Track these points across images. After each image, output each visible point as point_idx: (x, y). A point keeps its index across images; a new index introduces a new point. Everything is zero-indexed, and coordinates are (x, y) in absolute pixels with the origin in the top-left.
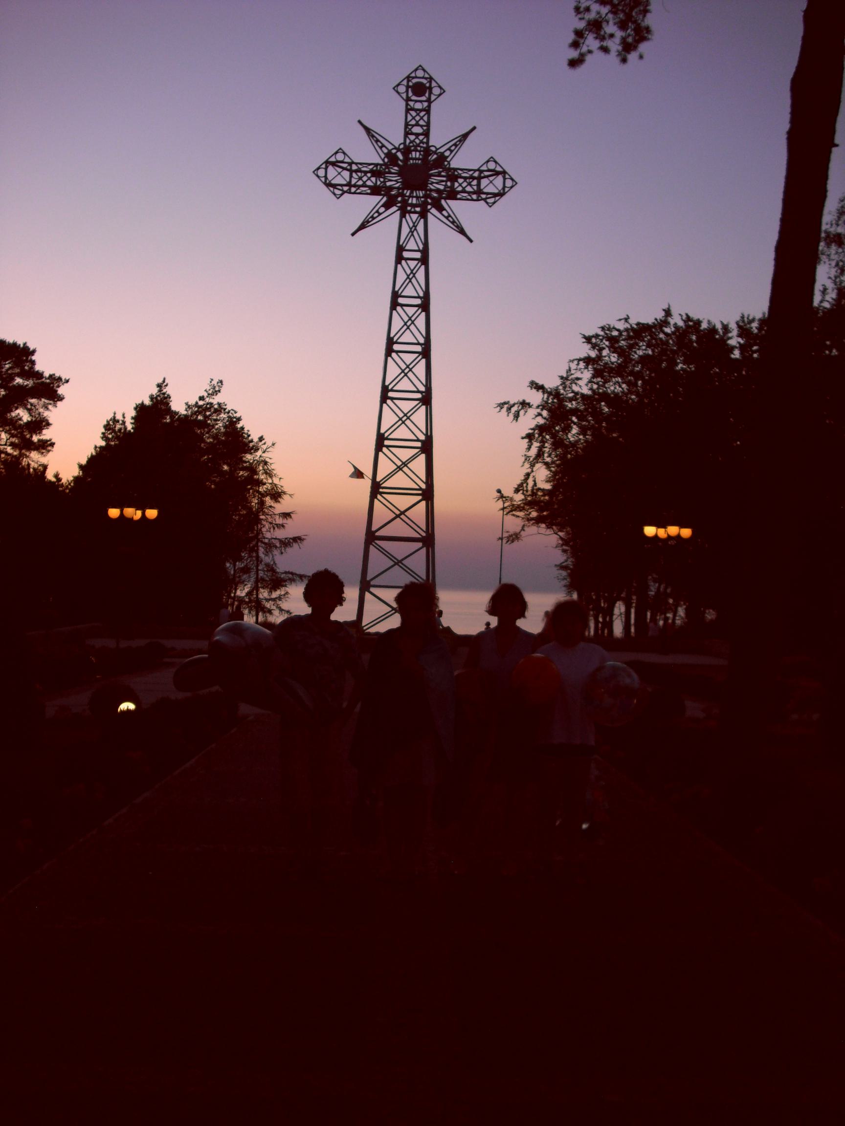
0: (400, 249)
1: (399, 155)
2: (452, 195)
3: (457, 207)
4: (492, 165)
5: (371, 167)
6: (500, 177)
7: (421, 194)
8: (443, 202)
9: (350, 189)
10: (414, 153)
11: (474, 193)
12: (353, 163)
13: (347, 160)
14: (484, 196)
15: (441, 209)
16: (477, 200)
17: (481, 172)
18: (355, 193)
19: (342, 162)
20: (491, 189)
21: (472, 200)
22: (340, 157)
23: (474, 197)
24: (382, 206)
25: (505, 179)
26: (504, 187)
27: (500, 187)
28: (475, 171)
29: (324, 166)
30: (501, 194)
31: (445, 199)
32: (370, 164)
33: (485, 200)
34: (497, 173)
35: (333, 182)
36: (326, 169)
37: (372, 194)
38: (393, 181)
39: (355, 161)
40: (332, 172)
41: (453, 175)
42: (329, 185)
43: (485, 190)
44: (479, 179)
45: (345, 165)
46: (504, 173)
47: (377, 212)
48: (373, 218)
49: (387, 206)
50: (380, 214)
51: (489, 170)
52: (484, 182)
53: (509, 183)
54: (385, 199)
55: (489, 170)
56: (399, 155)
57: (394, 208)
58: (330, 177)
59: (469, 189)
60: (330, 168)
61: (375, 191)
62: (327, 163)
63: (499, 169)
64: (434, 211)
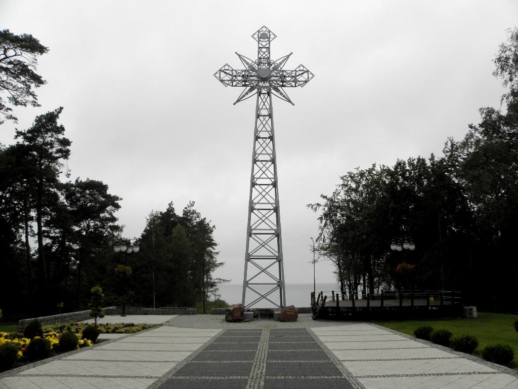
3: (287, 90)
4: (301, 68)
6: (306, 74)
12: (233, 70)
15: (277, 90)
16: (295, 86)
18: (236, 86)
19: (228, 70)
21: (292, 86)
22: (227, 67)
26: (308, 78)
30: (306, 82)
34: (305, 72)
40: (223, 74)
42: (222, 81)
45: (227, 72)
46: (308, 71)
53: (310, 76)
55: (300, 71)
58: (222, 77)
60: (222, 73)
62: (220, 70)
63: (305, 70)
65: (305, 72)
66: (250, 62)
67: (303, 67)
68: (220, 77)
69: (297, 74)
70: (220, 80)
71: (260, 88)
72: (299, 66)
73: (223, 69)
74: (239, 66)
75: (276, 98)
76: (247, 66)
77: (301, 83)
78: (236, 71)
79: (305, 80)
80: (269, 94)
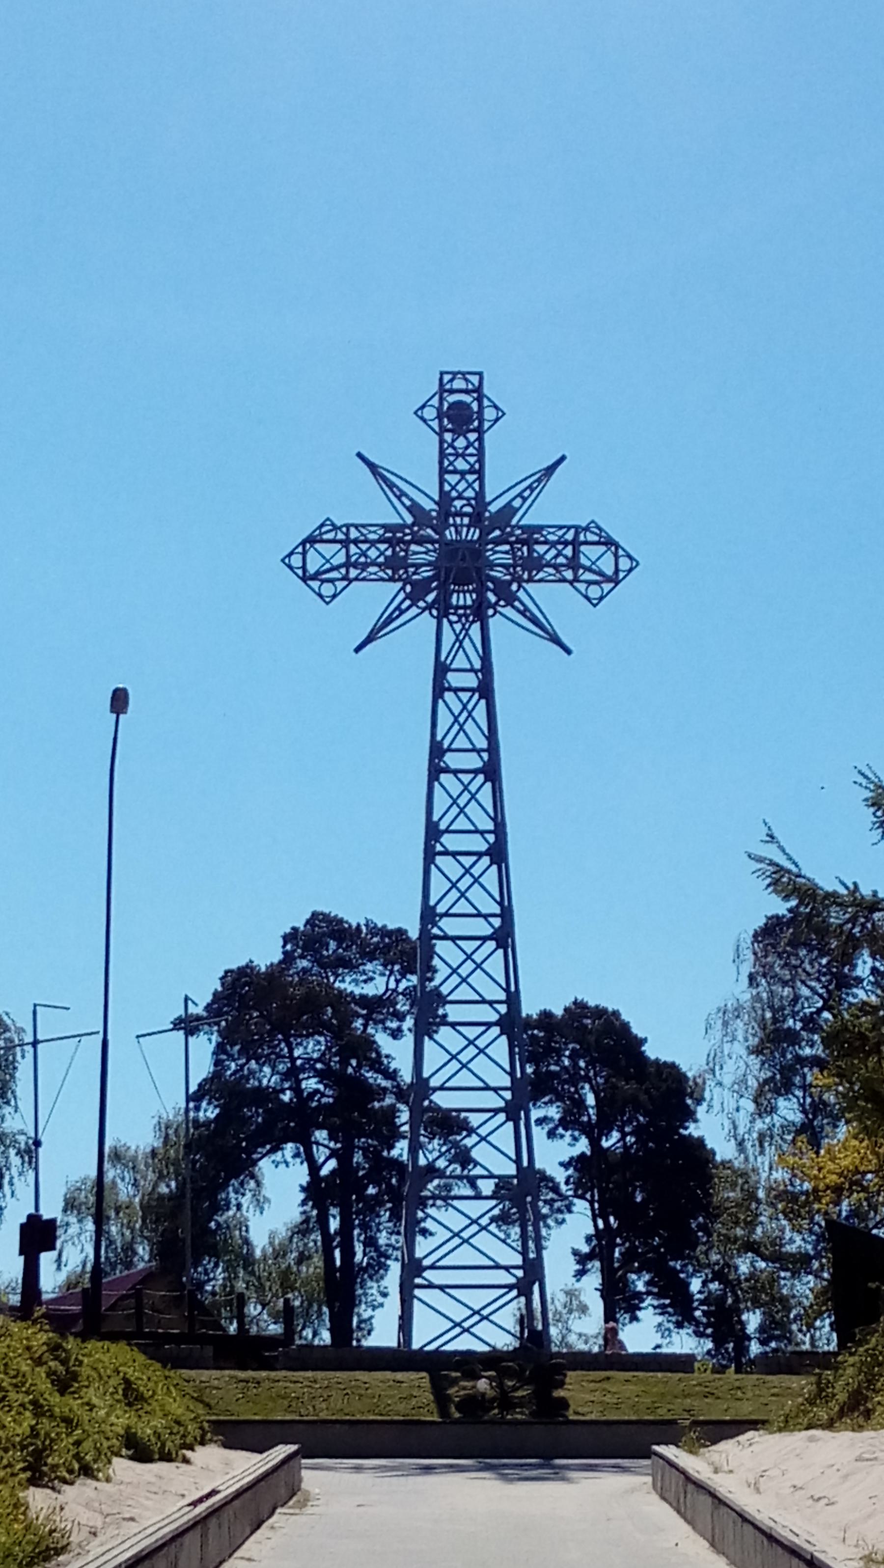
0: (441, 669)
1: (492, 598)
2: (393, 535)
3: (383, 512)
4: (327, 590)
5: (541, 575)
6: (312, 569)
7: (450, 534)
8: (409, 520)
9: (577, 534)
10: (469, 602)
11: (356, 542)
12: (571, 583)
13: (582, 587)
14: (341, 536)
15: (414, 508)
16: (348, 526)
18: (569, 528)
19: (590, 583)
20: (328, 550)
21: (356, 527)
22: (594, 592)
23: (354, 534)
24: (518, 509)
25: (304, 568)
26: (304, 554)
27: (311, 554)
28: (356, 579)
29: (621, 575)
30: (311, 540)
31: (404, 526)
32: (541, 580)
33: (335, 528)
35: (603, 548)
36: (617, 571)
37: (539, 529)
38: (500, 555)
39: (567, 585)
41: (395, 567)
42: (609, 543)
43: (339, 546)
44: (347, 565)
46: (305, 579)
47: (525, 499)
48: (530, 488)
49: (509, 510)
50: (520, 495)
51: (332, 581)
52: (341, 558)
53: (296, 561)
54: (514, 522)
55: (332, 581)
56: (492, 598)
57: (493, 508)
58: (609, 557)
59: (364, 547)
60: (609, 571)
61: (532, 535)
62: (615, 580)
63: (315, 584)
64: (428, 505)
65: (314, 577)
66: (508, 611)
67: (320, 596)
68: (616, 556)
69: (343, 571)
70: (617, 546)
71: (476, 519)
72: (334, 596)
73: (607, 587)
74: (548, 596)
75: (424, 483)
76: (521, 594)
77: (330, 536)
78: (564, 580)
79: (317, 546)
80: (445, 500)
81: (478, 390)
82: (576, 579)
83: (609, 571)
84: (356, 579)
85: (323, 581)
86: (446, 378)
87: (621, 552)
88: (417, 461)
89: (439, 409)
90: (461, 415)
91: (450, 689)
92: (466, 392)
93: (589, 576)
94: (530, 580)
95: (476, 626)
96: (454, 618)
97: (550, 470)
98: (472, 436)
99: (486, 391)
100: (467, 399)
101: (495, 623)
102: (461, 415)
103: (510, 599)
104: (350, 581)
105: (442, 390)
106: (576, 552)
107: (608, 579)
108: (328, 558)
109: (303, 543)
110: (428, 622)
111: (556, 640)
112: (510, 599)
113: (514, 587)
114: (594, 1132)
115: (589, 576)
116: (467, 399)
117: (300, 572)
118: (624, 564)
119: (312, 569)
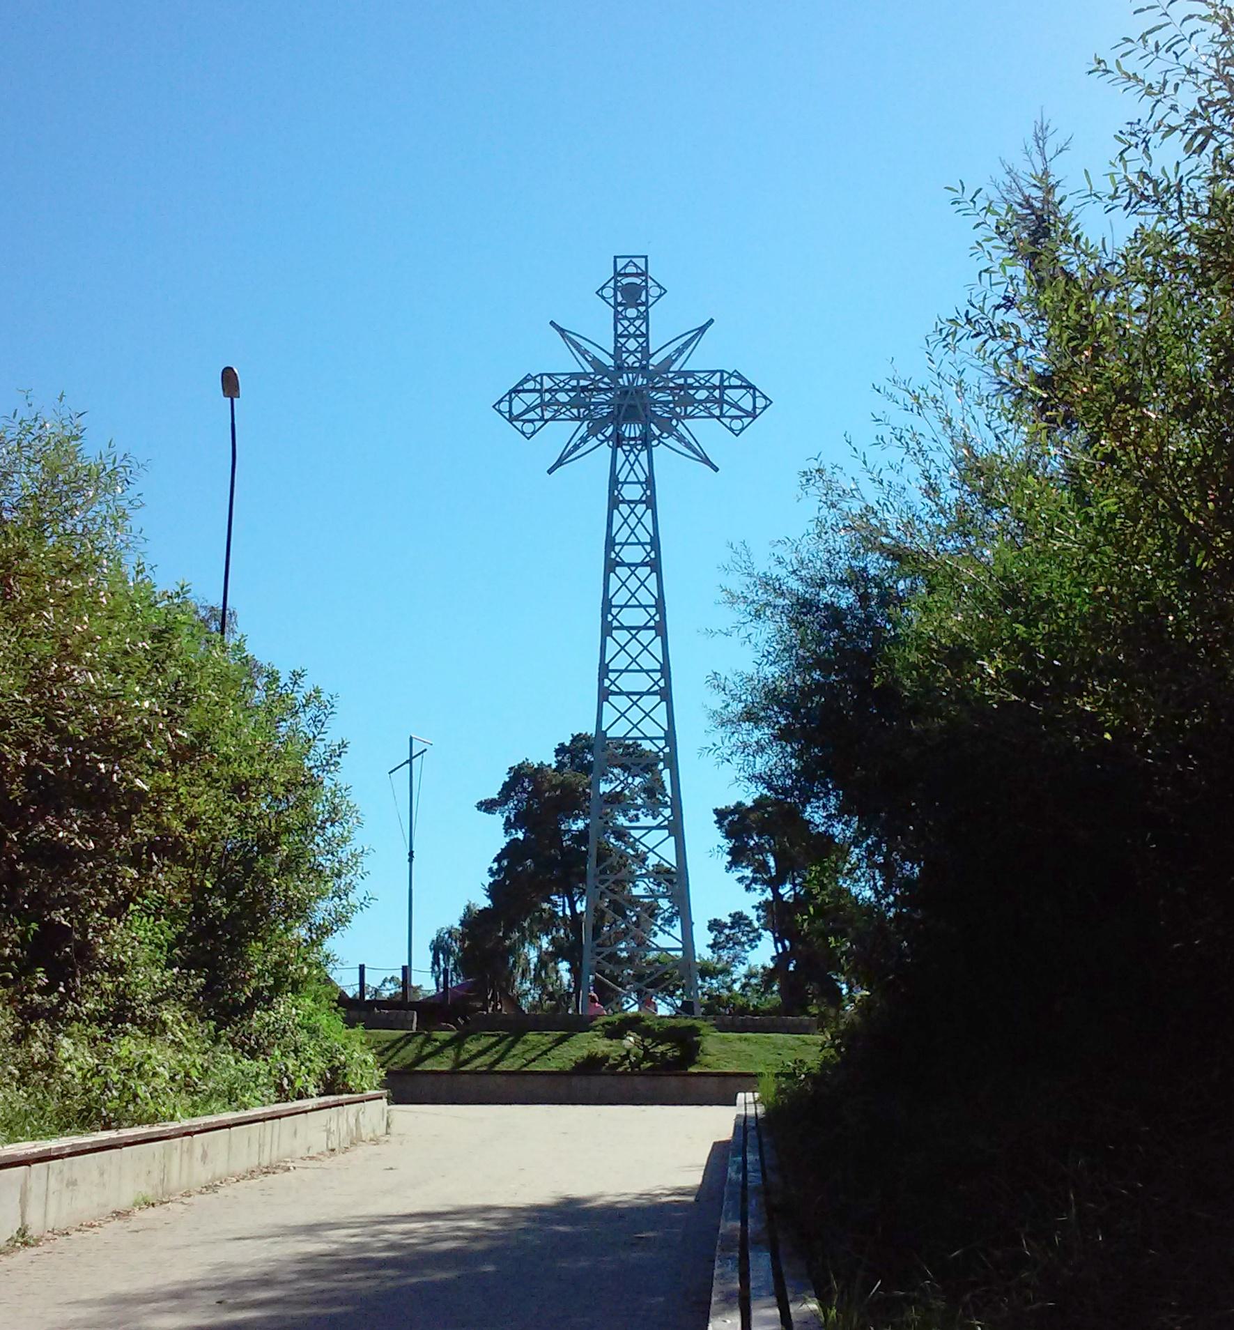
4: (528, 428)
6: (515, 412)
12: (718, 418)
15: (595, 362)
16: (542, 375)
17: (542, 418)
18: (714, 372)
21: (549, 375)
22: (737, 425)
25: (510, 411)
26: (510, 402)
27: (516, 401)
29: (758, 411)
30: (515, 391)
36: (755, 408)
40: (747, 404)
42: (750, 387)
46: (512, 419)
55: (532, 421)
58: (749, 397)
60: (750, 409)
63: (518, 424)
65: (517, 418)
66: (672, 441)
67: (523, 433)
68: (754, 398)
70: (755, 389)
74: (703, 429)
76: (680, 427)
78: (713, 416)
81: (645, 274)
82: (722, 415)
83: (750, 409)
84: (551, 419)
85: (525, 421)
86: (621, 263)
87: (758, 394)
88: (598, 327)
89: (615, 289)
90: (631, 291)
91: (623, 502)
92: (636, 275)
93: (734, 412)
94: (688, 416)
95: (644, 455)
96: (627, 448)
97: (702, 330)
98: (642, 309)
99: (649, 274)
100: (638, 281)
101: (659, 451)
102: (631, 291)
103: (671, 431)
104: (547, 421)
105: (617, 274)
106: (722, 394)
107: (748, 414)
108: (528, 403)
109: (510, 393)
110: (606, 450)
111: (706, 461)
112: (671, 431)
113: (674, 423)
114: (774, 884)
115: (734, 412)
116: (638, 281)
117: (507, 415)
118: (761, 403)
119: (515, 412)
